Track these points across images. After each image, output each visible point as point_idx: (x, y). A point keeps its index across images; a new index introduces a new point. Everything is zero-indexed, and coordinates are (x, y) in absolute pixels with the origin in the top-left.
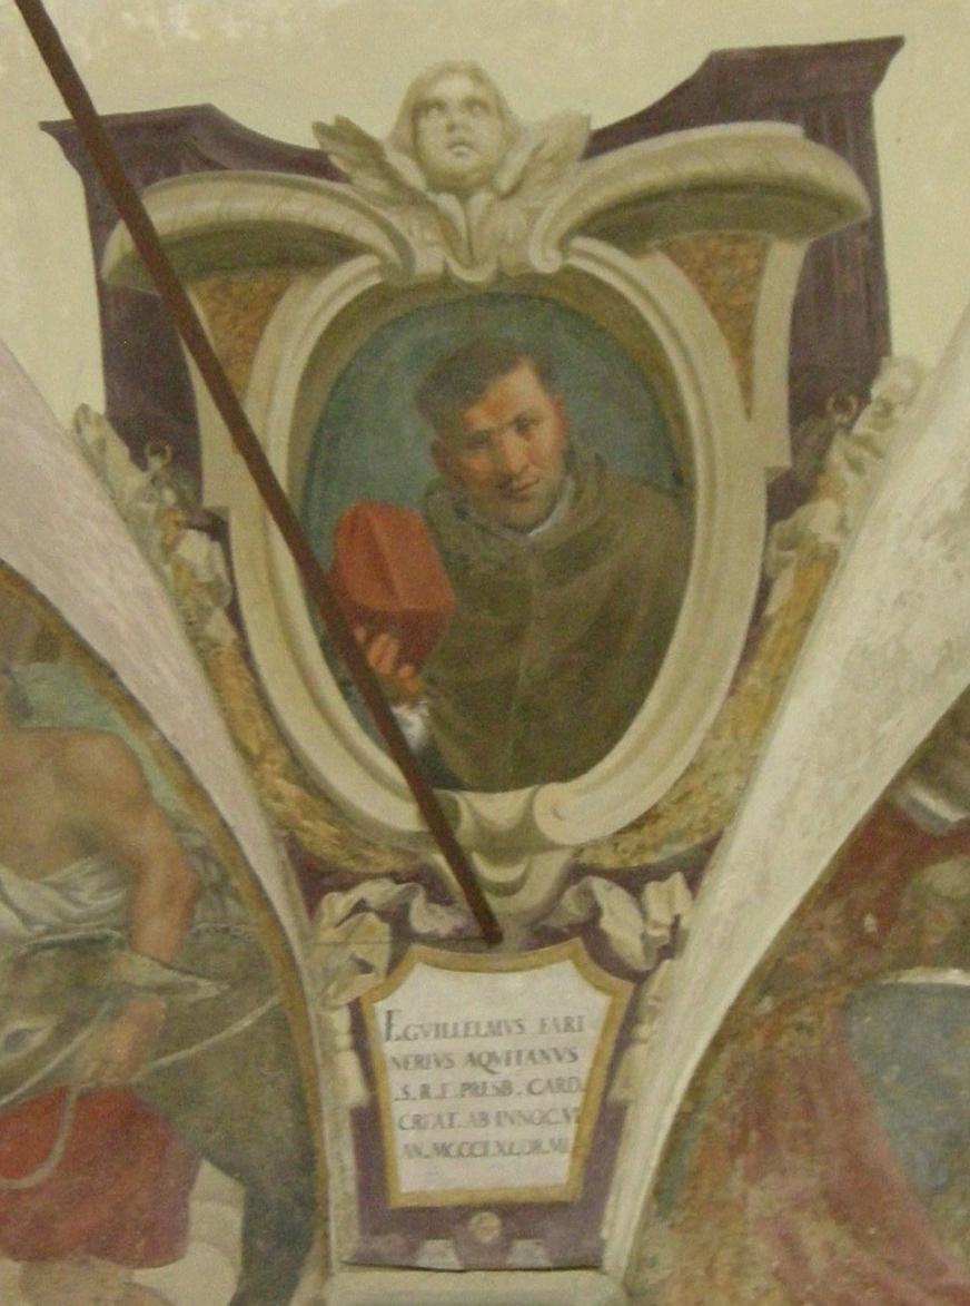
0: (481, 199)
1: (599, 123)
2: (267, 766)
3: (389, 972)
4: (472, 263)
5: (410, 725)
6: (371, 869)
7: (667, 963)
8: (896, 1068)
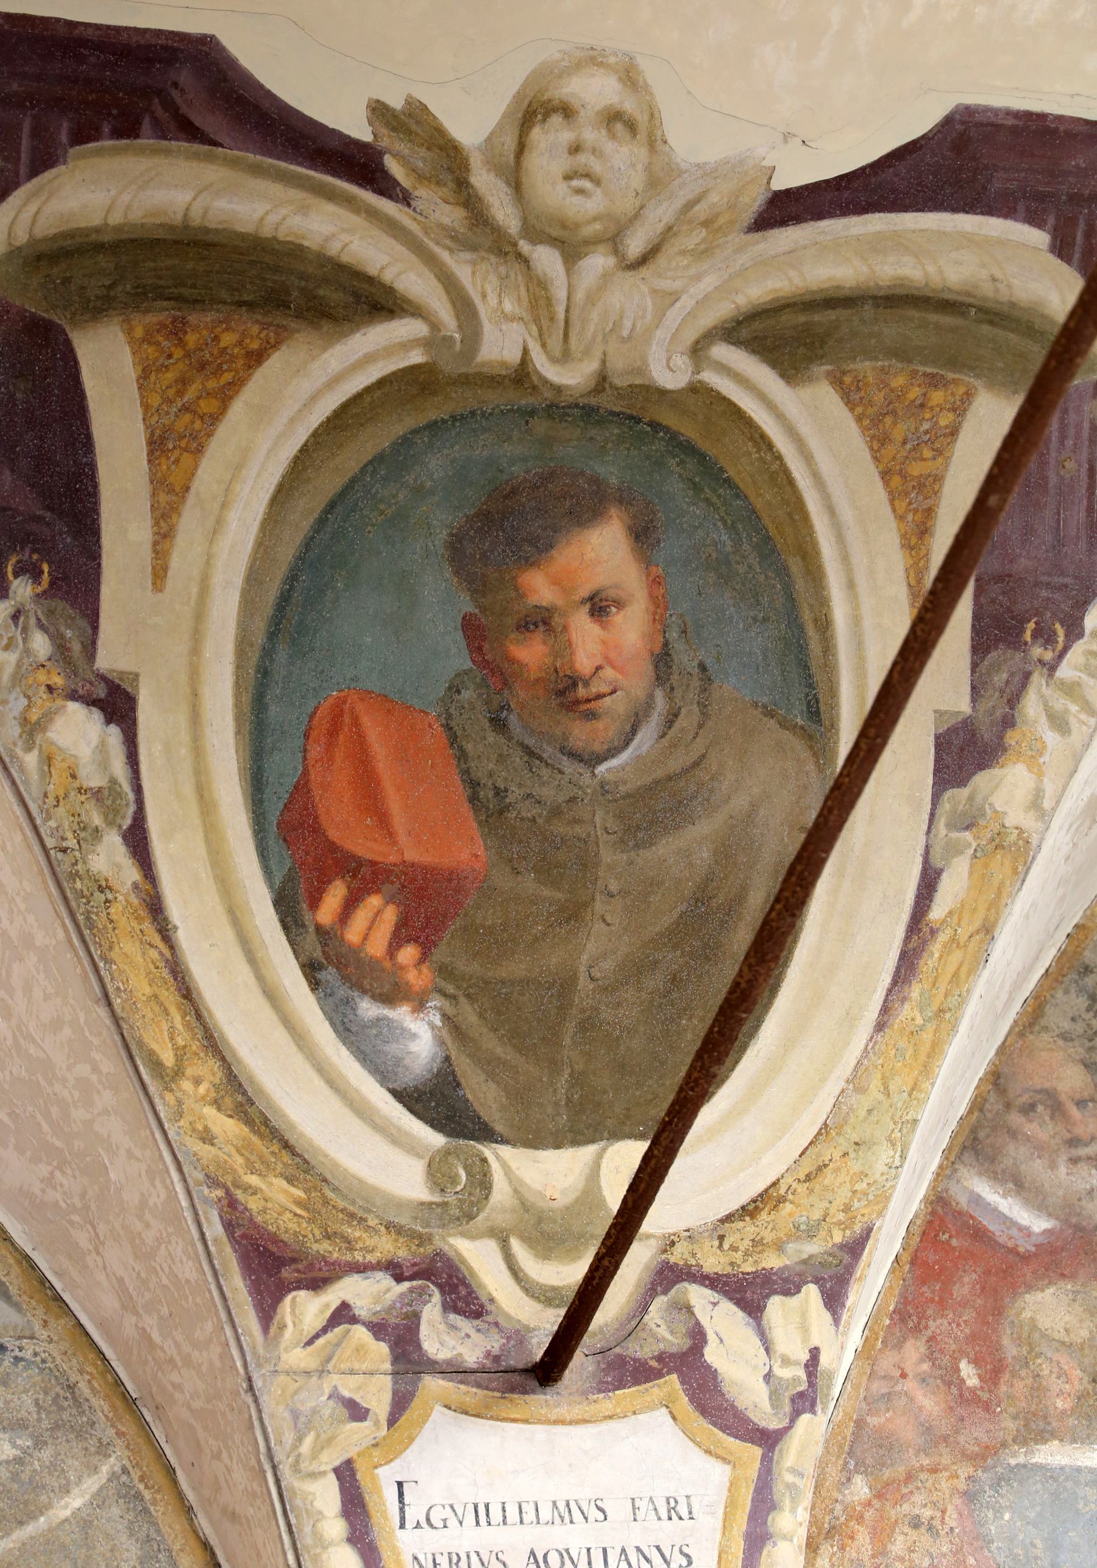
0: (598, 262)
1: (788, 178)
2: (186, 1085)
3: (392, 1422)
4: (565, 357)
5: (414, 1036)
6: (358, 1257)
7: (805, 1418)
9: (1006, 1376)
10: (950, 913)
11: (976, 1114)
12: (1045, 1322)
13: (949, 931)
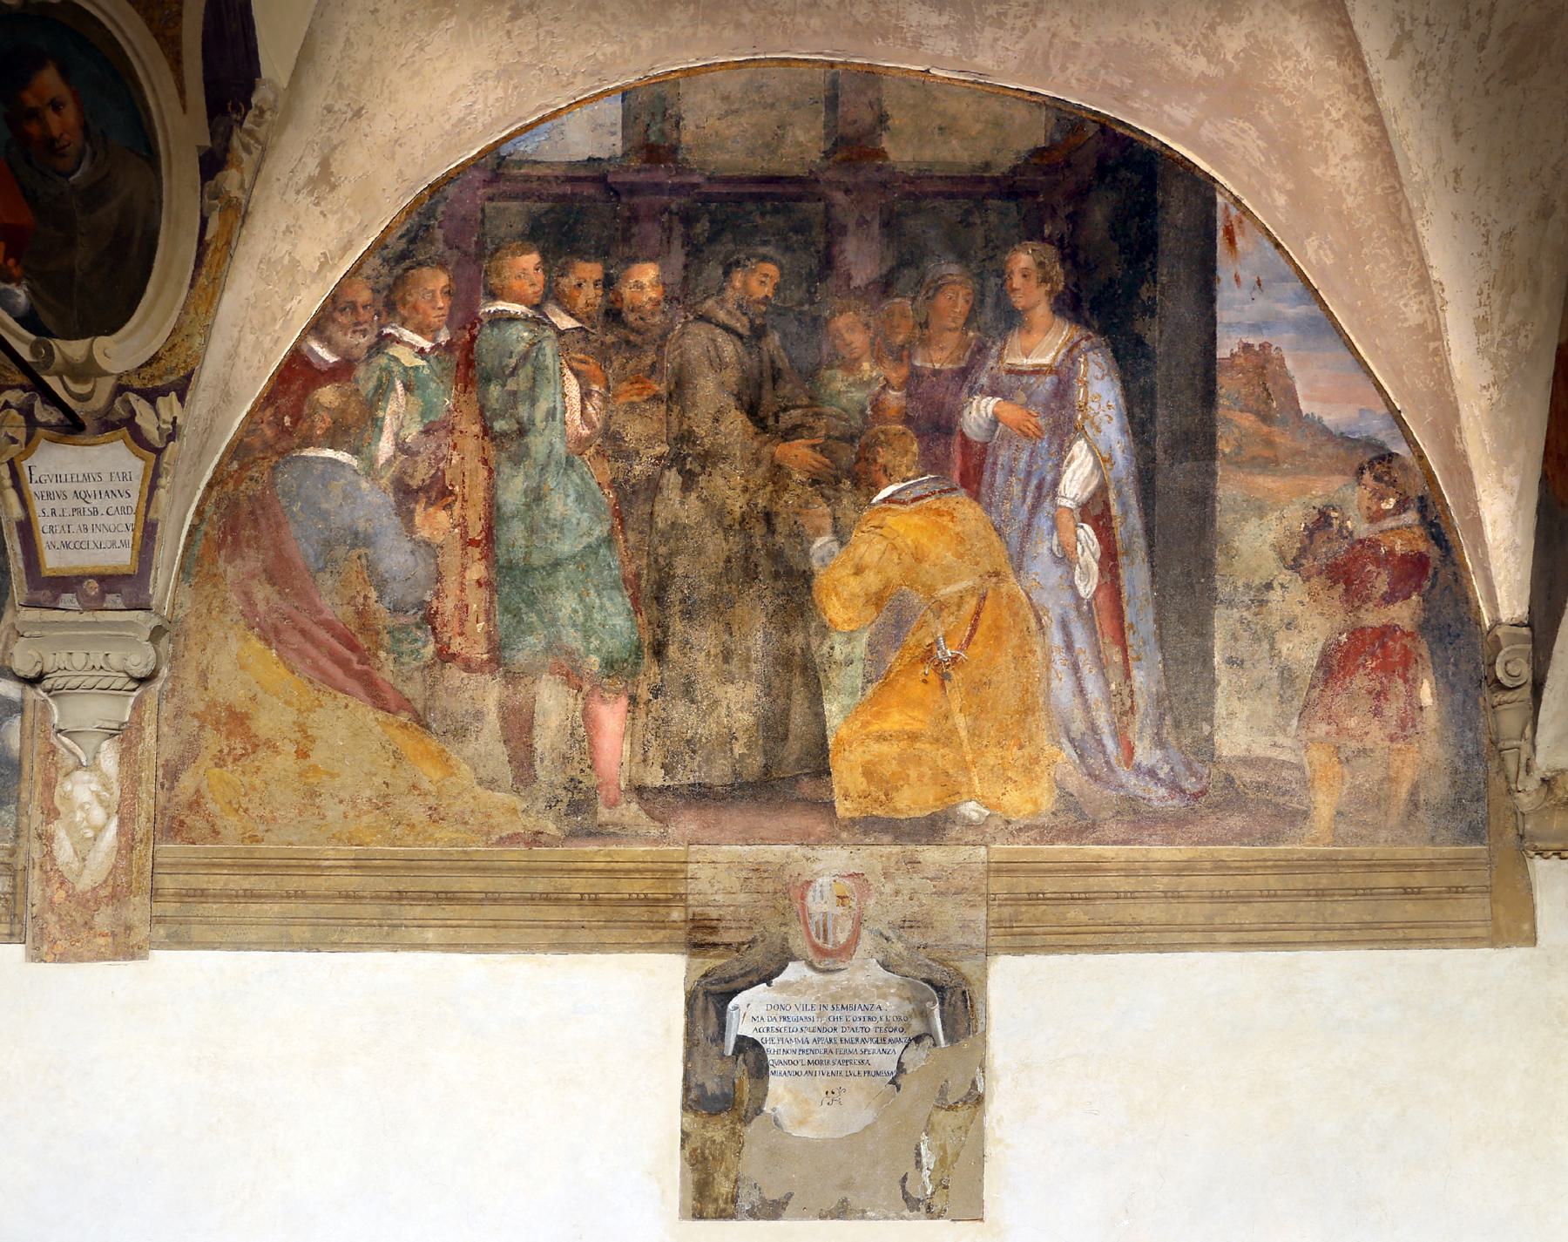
12: (322, 400)
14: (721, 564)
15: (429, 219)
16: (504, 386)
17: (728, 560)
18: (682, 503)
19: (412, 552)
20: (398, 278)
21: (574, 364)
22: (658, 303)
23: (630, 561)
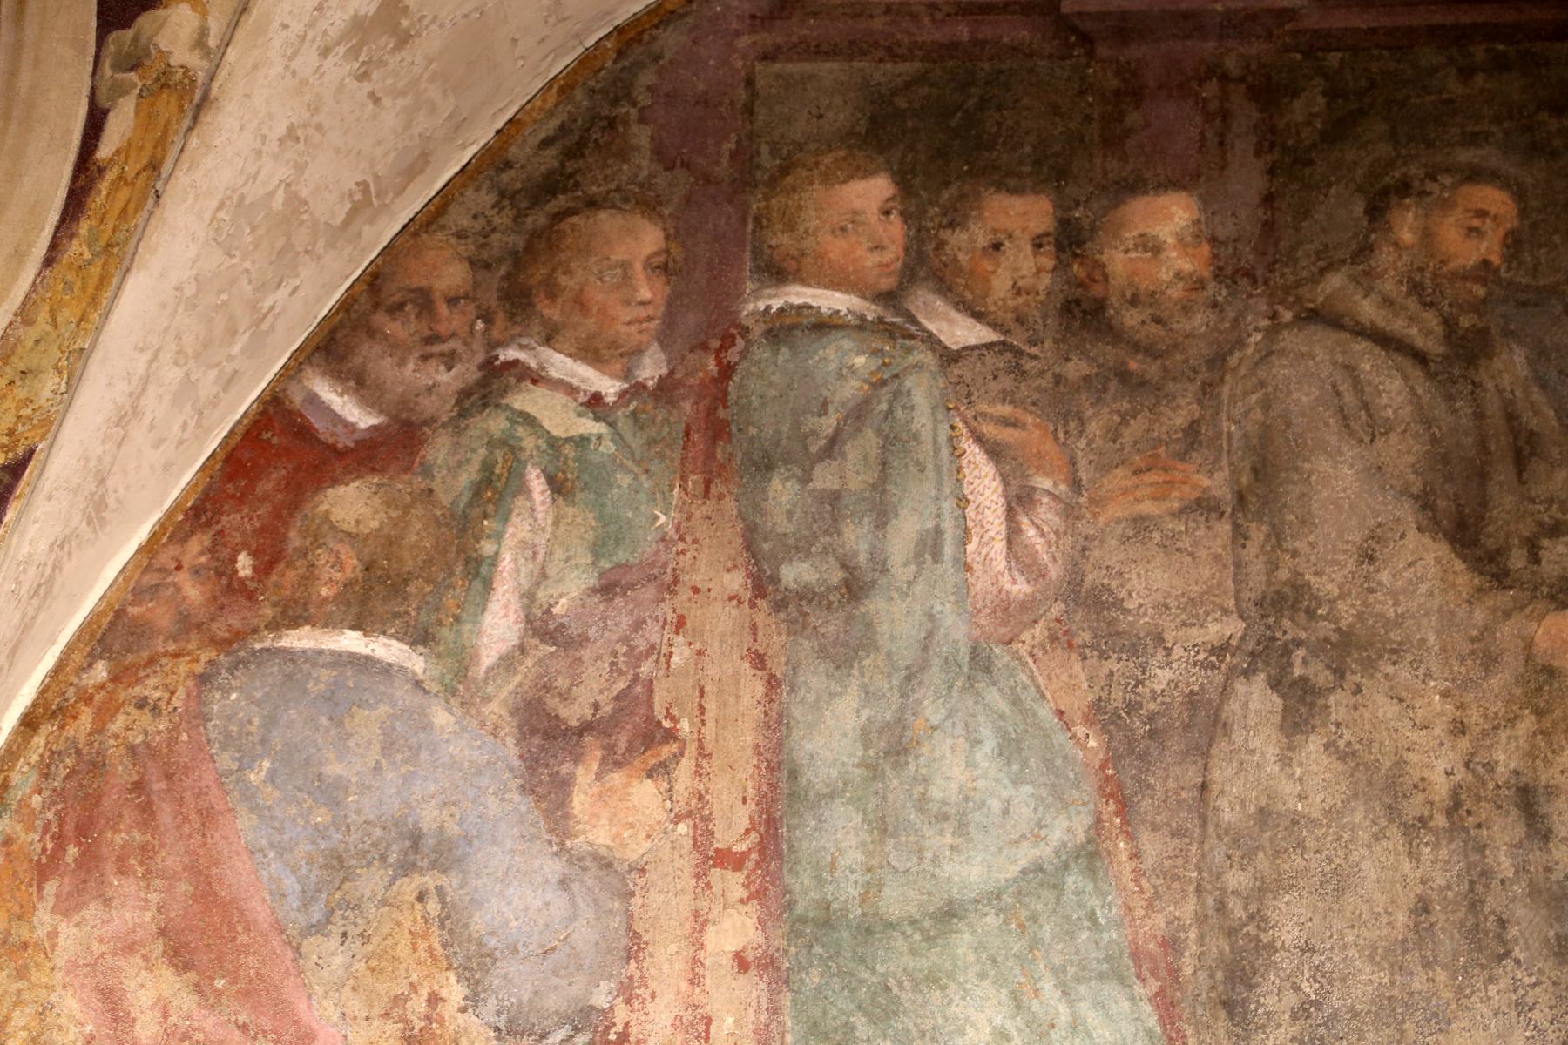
8: (266, 764)
9: (282, 566)
10: (118, 152)
11: (341, 315)
12: (338, 515)
13: (116, 169)
14: (1402, 918)
15: (615, 102)
16: (806, 479)
17: (1423, 907)
18: (1285, 761)
19: (564, 883)
20: (535, 234)
21: (987, 429)
22: (1200, 285)
23: (1150, 906)
